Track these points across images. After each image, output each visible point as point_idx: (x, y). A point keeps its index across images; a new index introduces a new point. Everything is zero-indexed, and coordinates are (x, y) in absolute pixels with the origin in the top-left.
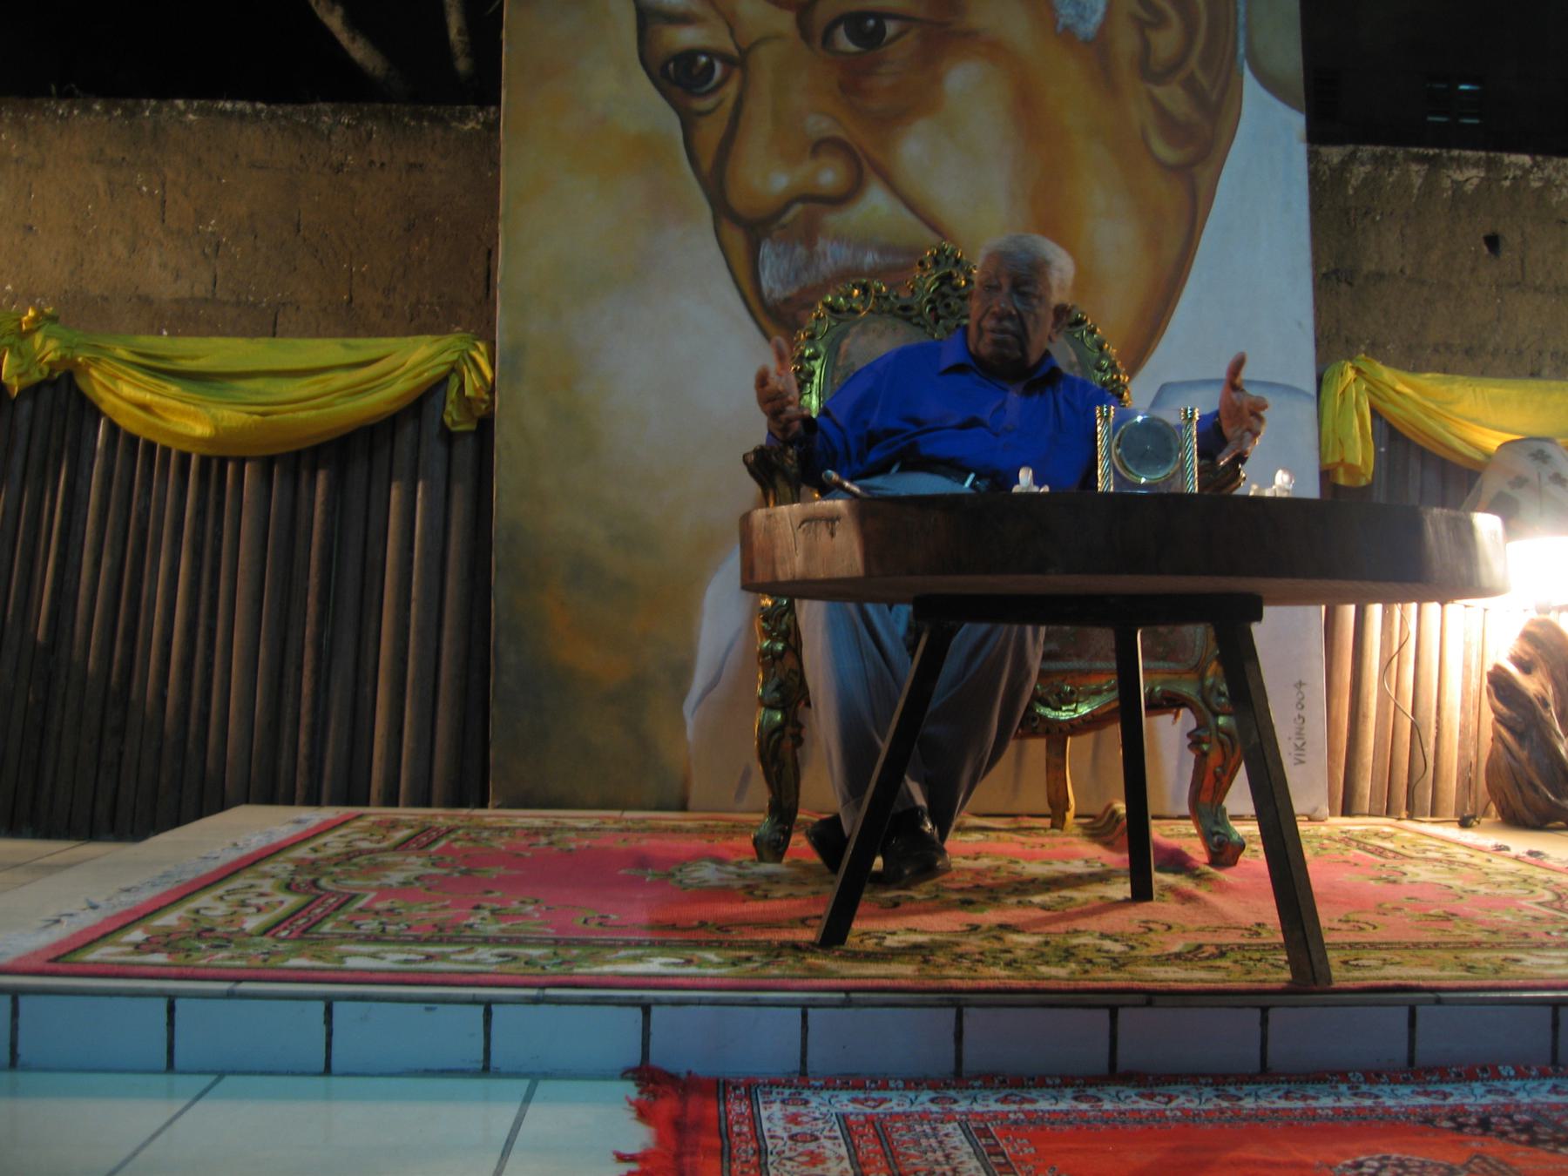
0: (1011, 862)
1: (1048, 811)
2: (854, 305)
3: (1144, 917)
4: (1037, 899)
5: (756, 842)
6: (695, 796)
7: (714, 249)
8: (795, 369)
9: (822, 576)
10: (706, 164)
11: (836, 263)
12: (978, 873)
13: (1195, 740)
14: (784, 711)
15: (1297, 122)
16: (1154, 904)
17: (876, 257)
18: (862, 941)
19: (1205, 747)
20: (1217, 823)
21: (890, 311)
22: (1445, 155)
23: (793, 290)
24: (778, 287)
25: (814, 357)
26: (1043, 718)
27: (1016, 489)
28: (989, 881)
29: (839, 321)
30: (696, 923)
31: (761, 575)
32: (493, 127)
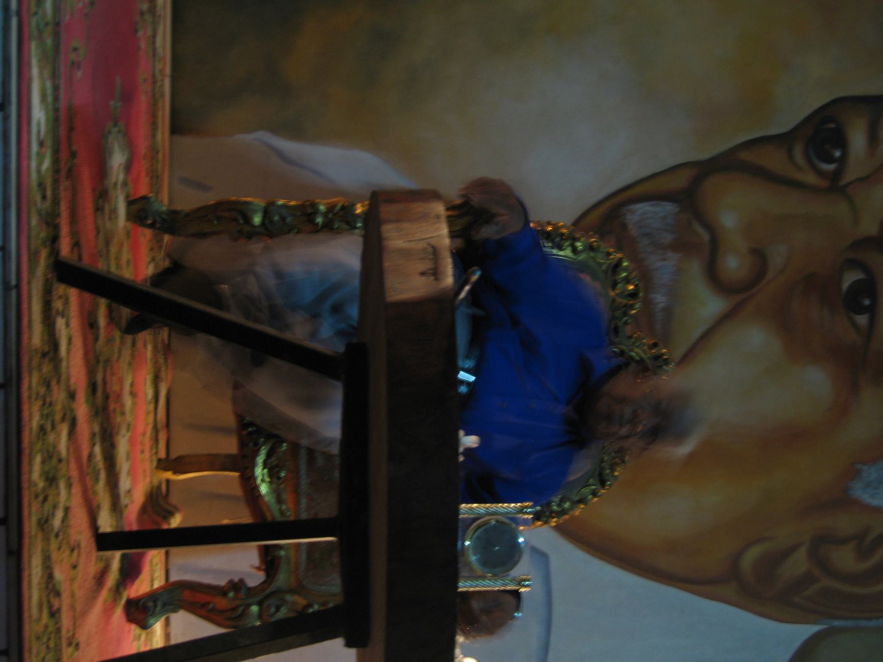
0: (129, 425)
1: (174, 455)
2: (620, 286)
3: (83, 544)
4: (97, 450)
5: (144, 198)
6: (186, 142)
7: (669, 162)
8: (562, 234)
9: (387, 264)
12: (119, 396)
13: (237, 586)
14: (263, 224)
16: (95, 554)
17: (662, 305)
18: (60, 297)
19: (231, 594)
20: (164, 605)
21: (613, 318)
23: (633, 231)
25: (575, 250)
26: (256, 453)
27: (461, 433)
28: (112, 406)
29: (606, 272)
30: (75, 148)
31: (386, 210)
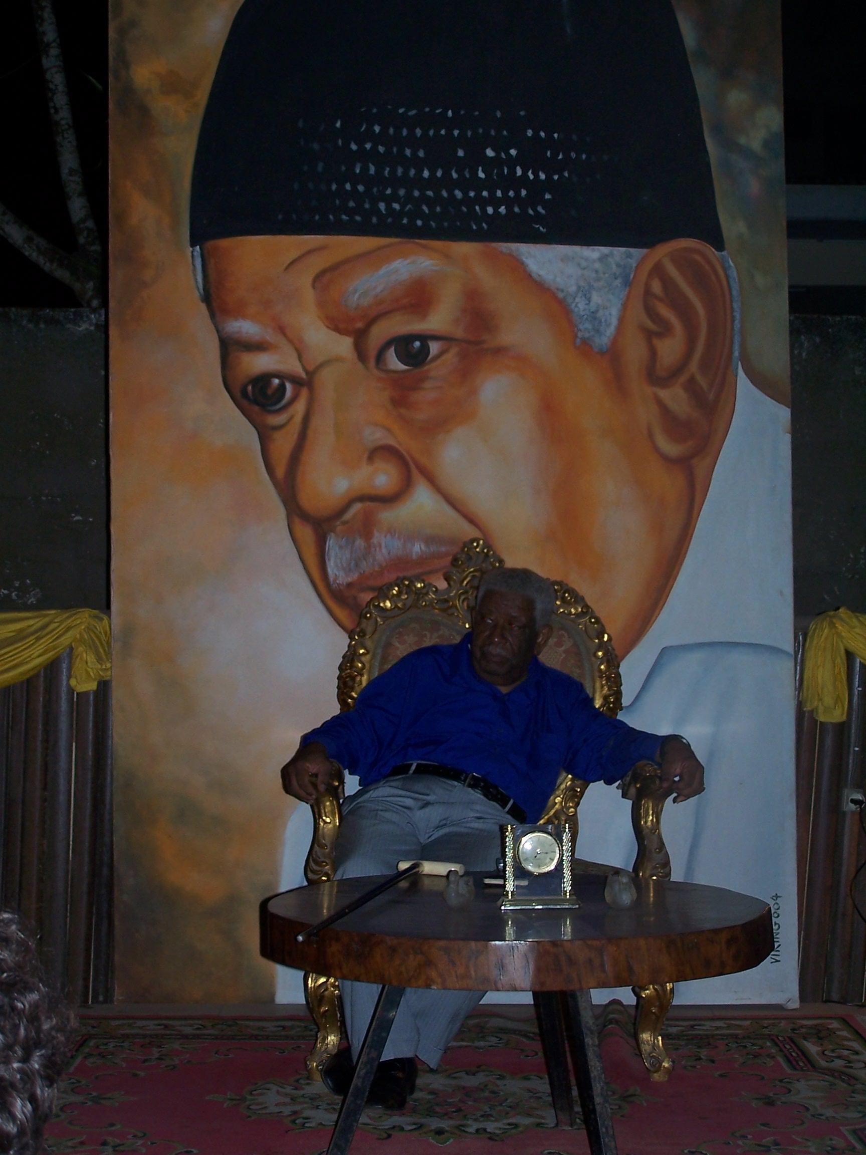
7: (288, 543)
10: (280, 472)
11: (389, 553)
15: (784, 414)
23: (354, 577)
24: (341, 574)
32: (105, 328)
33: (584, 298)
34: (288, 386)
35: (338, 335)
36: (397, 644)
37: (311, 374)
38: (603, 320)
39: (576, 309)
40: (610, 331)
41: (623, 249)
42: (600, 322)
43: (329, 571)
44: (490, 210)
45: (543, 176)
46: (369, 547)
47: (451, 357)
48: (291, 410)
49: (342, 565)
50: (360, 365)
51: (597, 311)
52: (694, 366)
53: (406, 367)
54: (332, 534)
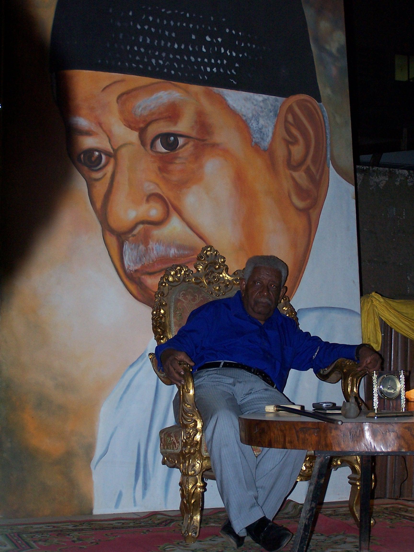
10: (99, 205)
22: (371, 169)
23: (138, 266)
24: (132, 264)
33: (255, 121)
34: (104, 157)
35: (130, 130)
36: (184, 300)
37: (116, 151)
38: (265, 134)
39: (252, 126)
40: (269, 139)
41: (274, 97)
42: (264, 134)
43: (125, 262)
44: (209, 69)
45: (234, 54)
46: (147, 249)
47: (190, 147)
48: (104, 171)
49: (132, 259)
50: (142, 147)
51: (262, 128)
52: (309, 161)
53: (167, 151)
54: (127, 241)
